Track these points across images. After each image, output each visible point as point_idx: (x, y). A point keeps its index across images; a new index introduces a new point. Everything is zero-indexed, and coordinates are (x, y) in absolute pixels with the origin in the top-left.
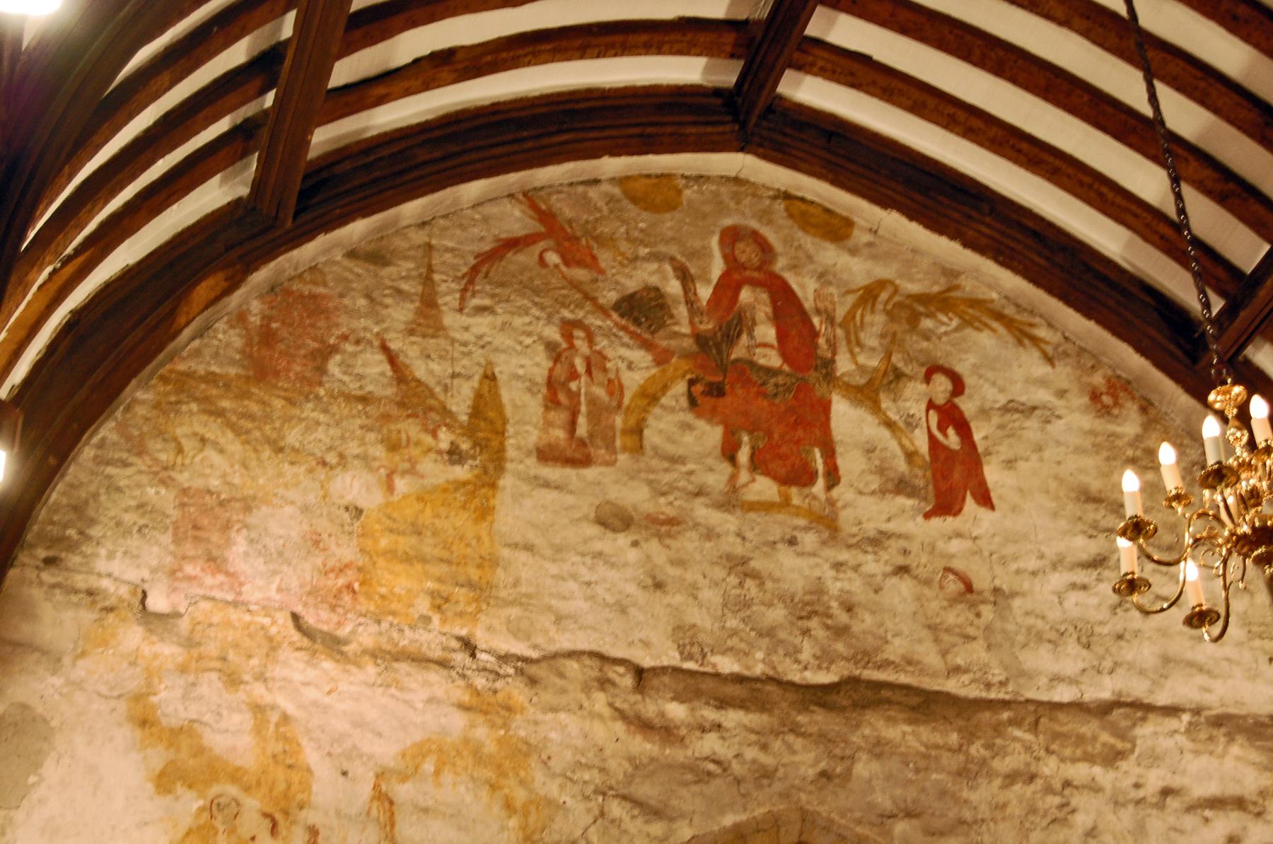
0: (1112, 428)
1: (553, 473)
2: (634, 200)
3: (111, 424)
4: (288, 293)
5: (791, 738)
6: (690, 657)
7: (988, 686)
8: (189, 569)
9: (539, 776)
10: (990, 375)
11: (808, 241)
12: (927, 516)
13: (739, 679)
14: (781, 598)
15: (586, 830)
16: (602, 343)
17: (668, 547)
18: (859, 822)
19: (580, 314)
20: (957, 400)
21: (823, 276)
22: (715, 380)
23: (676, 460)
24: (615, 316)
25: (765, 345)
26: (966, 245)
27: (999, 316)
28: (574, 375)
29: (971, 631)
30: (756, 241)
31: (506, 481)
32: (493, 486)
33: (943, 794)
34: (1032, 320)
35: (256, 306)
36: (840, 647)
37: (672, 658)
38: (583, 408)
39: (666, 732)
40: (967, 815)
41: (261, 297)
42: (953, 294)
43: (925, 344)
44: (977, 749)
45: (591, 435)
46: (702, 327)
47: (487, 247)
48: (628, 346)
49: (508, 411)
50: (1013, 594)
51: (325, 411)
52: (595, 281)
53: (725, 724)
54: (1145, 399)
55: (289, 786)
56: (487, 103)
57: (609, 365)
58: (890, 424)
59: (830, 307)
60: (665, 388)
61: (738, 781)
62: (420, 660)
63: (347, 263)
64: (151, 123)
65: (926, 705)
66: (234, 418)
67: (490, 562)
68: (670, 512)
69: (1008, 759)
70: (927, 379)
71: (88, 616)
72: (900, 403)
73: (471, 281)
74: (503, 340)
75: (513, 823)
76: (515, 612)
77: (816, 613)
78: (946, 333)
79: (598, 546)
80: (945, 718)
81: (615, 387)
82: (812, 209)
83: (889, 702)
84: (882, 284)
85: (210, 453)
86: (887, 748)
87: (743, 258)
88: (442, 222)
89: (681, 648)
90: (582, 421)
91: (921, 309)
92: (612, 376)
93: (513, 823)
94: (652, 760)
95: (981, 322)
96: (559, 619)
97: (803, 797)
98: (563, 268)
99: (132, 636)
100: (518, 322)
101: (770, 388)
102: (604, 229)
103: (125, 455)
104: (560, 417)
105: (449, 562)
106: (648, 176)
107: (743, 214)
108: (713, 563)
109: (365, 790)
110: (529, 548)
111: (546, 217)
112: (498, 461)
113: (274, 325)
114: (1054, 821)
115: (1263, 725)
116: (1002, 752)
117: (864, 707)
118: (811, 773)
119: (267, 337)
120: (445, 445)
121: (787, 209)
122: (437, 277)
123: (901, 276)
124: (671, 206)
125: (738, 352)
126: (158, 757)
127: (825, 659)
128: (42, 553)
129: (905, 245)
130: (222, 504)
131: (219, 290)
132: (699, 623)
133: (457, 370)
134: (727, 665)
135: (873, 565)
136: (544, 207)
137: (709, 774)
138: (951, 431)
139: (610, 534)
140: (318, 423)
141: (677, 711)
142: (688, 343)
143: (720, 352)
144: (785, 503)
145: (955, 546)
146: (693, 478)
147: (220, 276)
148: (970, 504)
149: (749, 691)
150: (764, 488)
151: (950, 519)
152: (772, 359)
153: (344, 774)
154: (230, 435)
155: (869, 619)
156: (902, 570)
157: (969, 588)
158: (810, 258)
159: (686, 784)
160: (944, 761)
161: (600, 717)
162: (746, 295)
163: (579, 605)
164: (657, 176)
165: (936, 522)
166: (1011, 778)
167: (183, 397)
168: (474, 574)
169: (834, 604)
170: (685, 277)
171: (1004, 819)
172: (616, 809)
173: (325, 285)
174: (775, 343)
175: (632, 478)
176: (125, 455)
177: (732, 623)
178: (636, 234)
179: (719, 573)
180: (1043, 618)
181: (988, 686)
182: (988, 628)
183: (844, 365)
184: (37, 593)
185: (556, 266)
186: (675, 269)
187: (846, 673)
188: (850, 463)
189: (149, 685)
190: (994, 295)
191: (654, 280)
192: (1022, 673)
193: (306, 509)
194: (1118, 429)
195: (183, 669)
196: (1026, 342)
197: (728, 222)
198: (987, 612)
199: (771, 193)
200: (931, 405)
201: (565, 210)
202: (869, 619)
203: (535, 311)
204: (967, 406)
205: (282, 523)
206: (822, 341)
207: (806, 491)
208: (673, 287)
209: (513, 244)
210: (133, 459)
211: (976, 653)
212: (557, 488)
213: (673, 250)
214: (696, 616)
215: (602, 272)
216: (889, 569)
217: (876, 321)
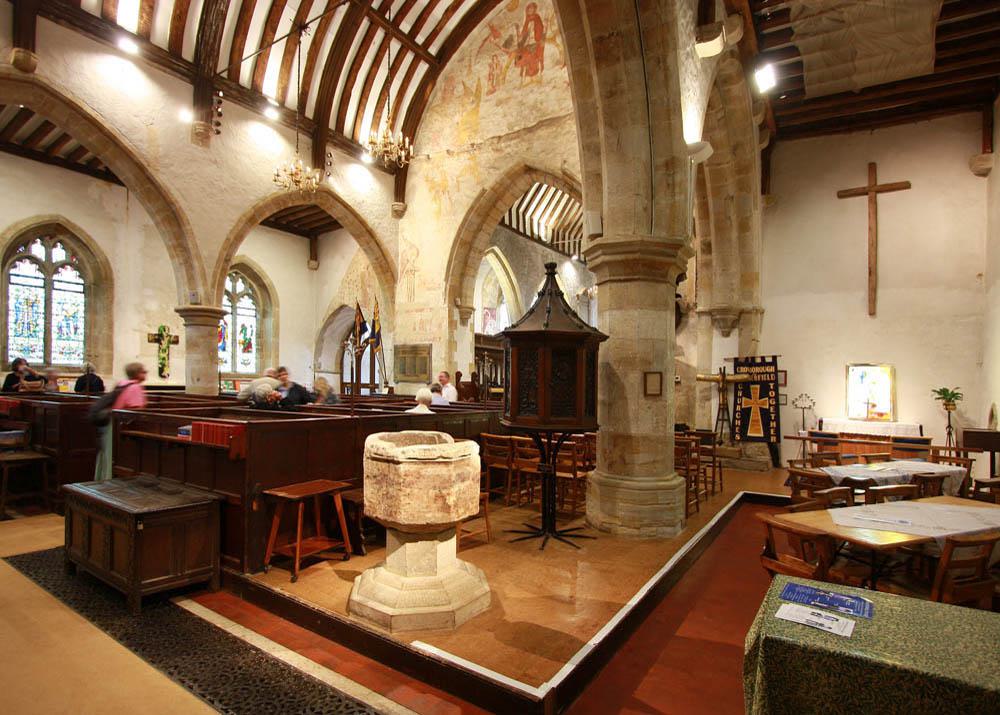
1: (489, 97)
31: (481, 103)
37: (507, 131)
44: (559, 129)
62: (463, 152)
110: (484, 118)
116: (562, 128)
119: (445, 90)
125: (526, 44)
134: (516, 129)
135: (548, 89)
149: (517, 135)
150: (528, 79)
156: (554, 87)
170: (517, 27)
172: (491, 170)
188: (547, 62)
205: (447, 131)
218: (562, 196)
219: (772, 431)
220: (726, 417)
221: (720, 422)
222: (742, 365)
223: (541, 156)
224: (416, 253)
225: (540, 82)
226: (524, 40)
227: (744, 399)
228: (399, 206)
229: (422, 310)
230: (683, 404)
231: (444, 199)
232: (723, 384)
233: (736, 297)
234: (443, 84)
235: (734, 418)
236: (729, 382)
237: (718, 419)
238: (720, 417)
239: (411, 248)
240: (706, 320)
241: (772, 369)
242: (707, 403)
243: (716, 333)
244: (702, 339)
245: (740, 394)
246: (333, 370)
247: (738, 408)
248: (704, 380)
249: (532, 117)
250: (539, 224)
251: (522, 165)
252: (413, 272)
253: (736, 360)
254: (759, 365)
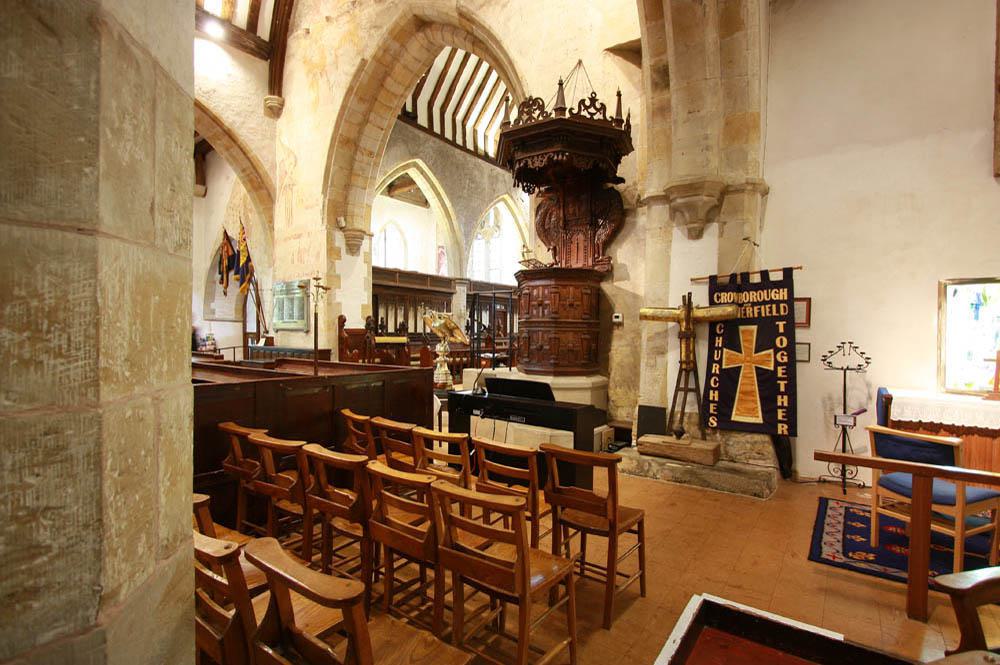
172: (373, 31)
218: (466, 57)
219: (780, 414)
220: (692, 385)
221: (681, 394)
222: (724, 288)
227: (725, 350)
229: (299, 236)
230: (626, 360)
232: (689, 326)
233: (715, 162)
235: (708, 387)
236: (698, 321)
237: (678, 389)
238: (682, 385)
240: (660, 211)
241: (783, 294)
242: (659, 359)
243: (678, 234)
244: (652, 245)
245: (719, 342)
246: (232, 317)
247: (715, 369)
248: (654, 318)
250: (485, 137)
251: (410, 16)
252: (291, 186)
253: (713, 279)
254: (756, 287)
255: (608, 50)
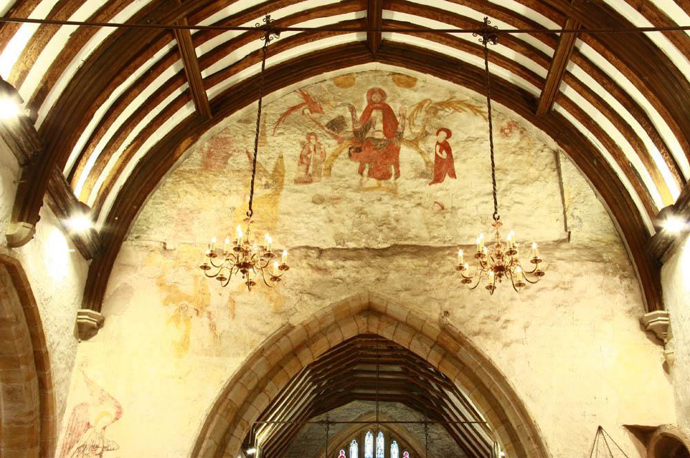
0: (507, 141)
1: (300, 187)
2: (338, 85)
3: (158, 191)
4: (218, 138)
5: (368, 268)
6: (339, 244)
7: (445, 242)
8: (180, 234)
9: (282, 289)
10: (462, 129)
11: (399, 89)
12: (430, 184)
13: (355, 249)
14: (373, 220)
15: (295, 305)
16: (320, 139)
17: (336, 207)
18: (388, 294)
19: (314, 130)
20: (447, 140)
21: (403, 102)
22: (360, 145)
23: (342, 177)
24: (326, 128)
25: (379, 131)
26: (454, 82)
27: (469, 106)
28: (309, 152)
29: (441, 223)
30: (380, 93)
31: (284, 192)
32: (279, 194)
33: (419, 281)
34: (481, 105)
35: (206, 144)
36: (392, 234)
37: (333, 245)
38: (312, 163)
39: (325, 270)
40: (428, 288)
41: (208, 141)
42: (452, 100)
43: (439, 121)
44: (434, 265)
45: (314, 172)
46: (357, 128)
47: (284, 111)
48: (329, 139)
49: (286, 169)
50: (459, 208)
51: (226, 177)
52: (321, 117)
53: (346, 266)
54: (523, 128)
55: (203, 300)
56: (279, 63)
57: (322, 147)
58: (421, 153)
59: (404, 112)
60: (341, 152)
61: (348, 284)
63: (238, 124)
64: (144, 101)
65: (419, 251)
66: (196, 183)
67: (276, 220)
68: (338, 195)
69: (445, 267)
70: (437, 134)
71: (145, 254)
72: (427, 144)
73: (278, 125)
74: (287, 144)
75: (272, 305)
76: (282, 235)
77: (385, 224)
78: (447, 116)
79: (312, 210)
80: (424, 256)
81: (323, 154)
82: (402, 77)
83: (405, 252)
84: (425, 101)
85: (188, 196)
86: (401, 268)
87: (374, 100)
88: (271, 104)
89: (336, 241)
90: (311, 168)
91: (440, 108)
92: (322, 150)
93: (272, 305)
94: (320, 280)
95: (461, 109)
96: (296, 237)
97: (370, 287)
98: (310, 114)
99: (158, 258)
100: (292, 136)
101: (378, 146)
102: (326, 98)
103: (162, 200)
104: (303, 167)
105: (262, 222)
106: (344, 75)
107: (377, 83)
108: (351, 211)
109: (226, 299)
110: (288, 214)
111: (306, 97)
112: (281, 186)
113: (212, 150)
114: (458, 287)
115: (549, 245)
116: (444, 265)
117: (395, 255)
118: (373, 279)
119: (209, 154)
120: (264, 183)
121: (393, 79)
122: (266, 125)
123: (434, 96)
124: (350, 85)
125: (368, 135)
126: (165, 295)
127: (386, 239)
128: (135, 235)
129: (434, 86)
130: (191, 212)
131: (190, 143)
132: (344, 232)
133: (271, 156)
134: (352, 245)
135: (407, 204)
136: (306, 93)
137: (338, 283)
138: (444, 152)
139: (316, 206)
140: (223, 181)
141: (330, 263)
142: (351, 135)
143: (362, 136)
144: (380, 186)
145: (439, 194)
146: (347, 182)
147: (190, 138)
148: (447, 178)
149: (357, 253)
150: (373, 182)
151: (438, 184)
152: (380, 135)
153: (220, 294)
154: (195, 189)
155: (404, 223)
156: (419, 204)
157: (443, 208)
158: (399, 95)
159: (329, 287)
160: (421, 271)
161: (303, 268)
162: (374, 113)
163: (304, 231)
164: (347, 75)
165: (433, 186)
166: (445, 274)
167: (181, 179)
168: (270, 225)
169: (392, 220)
170: (353, 110)
171: (441, 288)
172: (306, 297)
173: (229, 133)
174: (382, 129)
175: (326, 185)
176: (162, 200)
177: (355, 231)
178: (338, 97)
179: (352, 214)
180: (469, 215)
181: (445, 242)
182: (448, 222)
183: (407, 134)
184: (131, 248)
185: (308, 114)
186: (350, 108)
187: (393, 243)
188: (405, 169)
189: (163, 273)
190: (468, 98)
191: (341, 113)
192: (458, 236)
193: (218, 210)
194: (510, 141)
195: (174, 267)
196: (478, 114)
197: (371, 87)
198: (448, 216)
199: (388, 74)
200: (438, 143)
201: (312, 92)
202: (404, 223)
203: (298, 132)
204: (451, 141)
206: (399, 126)
207: (386, 181)
208: (348, 115)
209: (294, 108)
210: (165, 201)
211: (443, 231)
212: (300, 192)
213: (350, 101)
214: (343, 230)
215: (324, 113)
216: (414, 205)
217: (422, 114)
223: (403, 294)
224: (113, 411)
225: (393, 192)
226: (366, 128)
228: (89, 317)
231: (200, 326)
234: (206, 144)
239: (102, 400)
249: (381, 236)
251: (365, 301)
255: (625, 426)
